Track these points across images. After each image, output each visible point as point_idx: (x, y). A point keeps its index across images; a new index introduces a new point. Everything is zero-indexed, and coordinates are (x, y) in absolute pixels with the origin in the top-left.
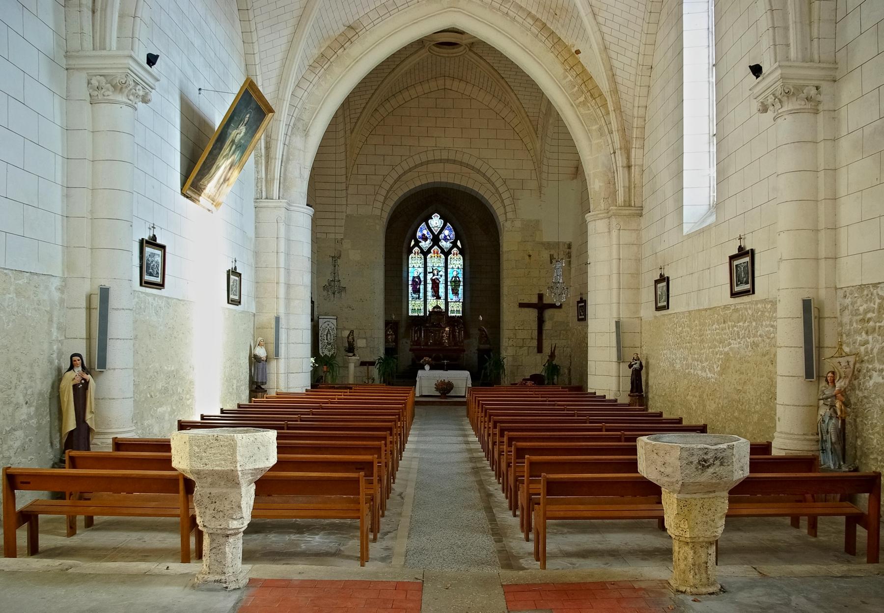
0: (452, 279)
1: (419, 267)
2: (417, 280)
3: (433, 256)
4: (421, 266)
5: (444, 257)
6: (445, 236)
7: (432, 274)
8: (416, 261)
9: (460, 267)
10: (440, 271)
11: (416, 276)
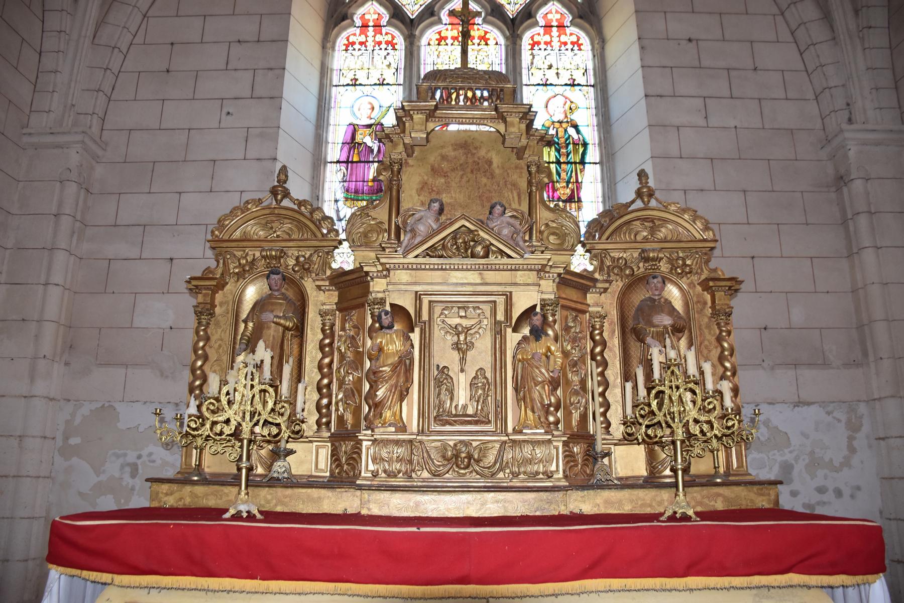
2: (368, 141)
5: (502, 40)
9: (580, 79)
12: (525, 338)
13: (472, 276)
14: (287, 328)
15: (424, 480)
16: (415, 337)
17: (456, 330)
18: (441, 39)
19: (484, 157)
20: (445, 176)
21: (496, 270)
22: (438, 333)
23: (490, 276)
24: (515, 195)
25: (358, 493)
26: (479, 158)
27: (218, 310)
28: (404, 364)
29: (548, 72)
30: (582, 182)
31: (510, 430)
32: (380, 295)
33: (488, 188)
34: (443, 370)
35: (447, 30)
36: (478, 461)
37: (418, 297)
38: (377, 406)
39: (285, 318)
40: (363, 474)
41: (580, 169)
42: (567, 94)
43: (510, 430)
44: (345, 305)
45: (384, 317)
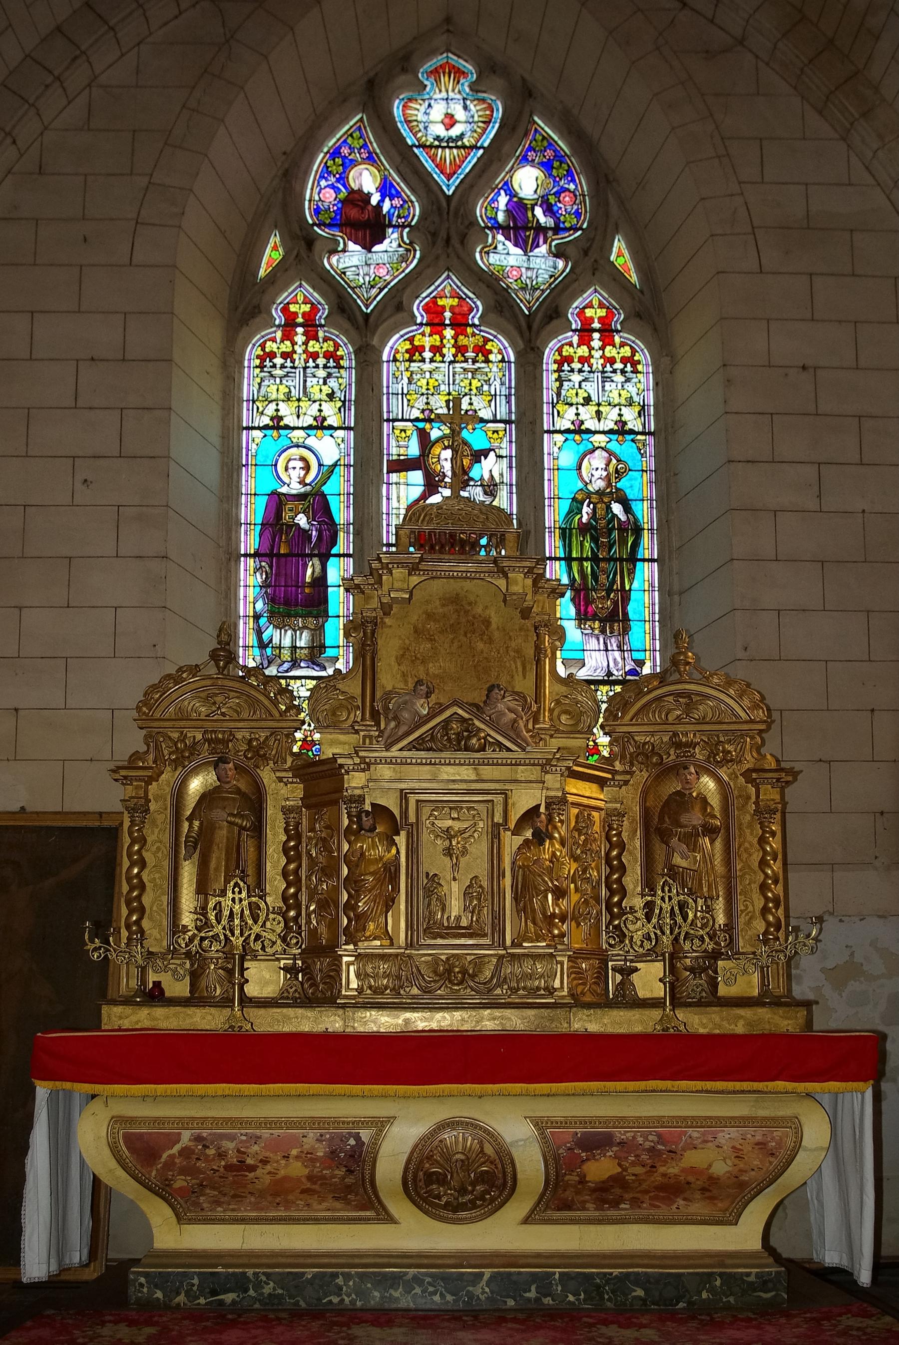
0: (577, 503)
1: (320, 425)
2: (302, 520)
3: (427, 342)
4: (333, 420)
6: (518, 207)
7: (417, 477)
8: (295, 383)
10: (479, 456)
11: (296, 488)
12: (527, 841)
13: (465, 772)
14: (244, 829)
15: (414, 997)
16: (401, 840)
17: (448, 834)
18: (415, 351)
19: (480, 616)
20: (431, 640)
21: (493, 765)
22: (426, 837)
23: (487, 772)
24: (519, 664)
25: (340, 1012)
26: (474, 617)
27: (153, 806)
28: (391, 872)
29: (581, 409)
30: (630, 590)
31: (508, 942)
32: (358, 792)
33: (485, 655)
34: (433, 879)
35: (423, 334)
36: (473, 977)
37: (404, 796)
38: (361, 919)
39: (242, 817)
40: (343, 993)
41: (628, 570)
42: (614, 446)
43: (508, 942)
44: (313, 800)
45: (364, 819)
